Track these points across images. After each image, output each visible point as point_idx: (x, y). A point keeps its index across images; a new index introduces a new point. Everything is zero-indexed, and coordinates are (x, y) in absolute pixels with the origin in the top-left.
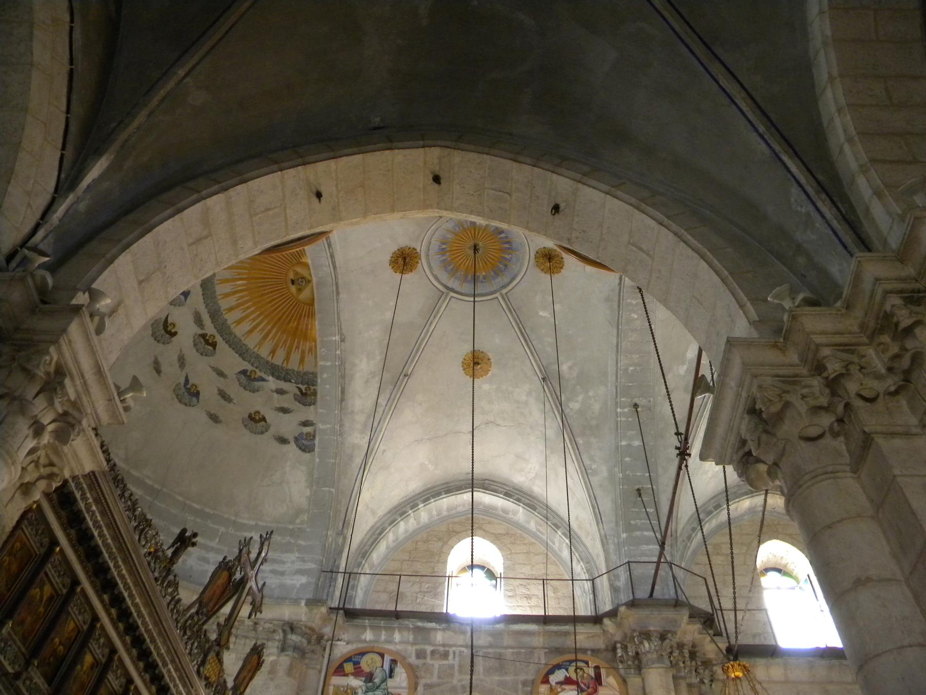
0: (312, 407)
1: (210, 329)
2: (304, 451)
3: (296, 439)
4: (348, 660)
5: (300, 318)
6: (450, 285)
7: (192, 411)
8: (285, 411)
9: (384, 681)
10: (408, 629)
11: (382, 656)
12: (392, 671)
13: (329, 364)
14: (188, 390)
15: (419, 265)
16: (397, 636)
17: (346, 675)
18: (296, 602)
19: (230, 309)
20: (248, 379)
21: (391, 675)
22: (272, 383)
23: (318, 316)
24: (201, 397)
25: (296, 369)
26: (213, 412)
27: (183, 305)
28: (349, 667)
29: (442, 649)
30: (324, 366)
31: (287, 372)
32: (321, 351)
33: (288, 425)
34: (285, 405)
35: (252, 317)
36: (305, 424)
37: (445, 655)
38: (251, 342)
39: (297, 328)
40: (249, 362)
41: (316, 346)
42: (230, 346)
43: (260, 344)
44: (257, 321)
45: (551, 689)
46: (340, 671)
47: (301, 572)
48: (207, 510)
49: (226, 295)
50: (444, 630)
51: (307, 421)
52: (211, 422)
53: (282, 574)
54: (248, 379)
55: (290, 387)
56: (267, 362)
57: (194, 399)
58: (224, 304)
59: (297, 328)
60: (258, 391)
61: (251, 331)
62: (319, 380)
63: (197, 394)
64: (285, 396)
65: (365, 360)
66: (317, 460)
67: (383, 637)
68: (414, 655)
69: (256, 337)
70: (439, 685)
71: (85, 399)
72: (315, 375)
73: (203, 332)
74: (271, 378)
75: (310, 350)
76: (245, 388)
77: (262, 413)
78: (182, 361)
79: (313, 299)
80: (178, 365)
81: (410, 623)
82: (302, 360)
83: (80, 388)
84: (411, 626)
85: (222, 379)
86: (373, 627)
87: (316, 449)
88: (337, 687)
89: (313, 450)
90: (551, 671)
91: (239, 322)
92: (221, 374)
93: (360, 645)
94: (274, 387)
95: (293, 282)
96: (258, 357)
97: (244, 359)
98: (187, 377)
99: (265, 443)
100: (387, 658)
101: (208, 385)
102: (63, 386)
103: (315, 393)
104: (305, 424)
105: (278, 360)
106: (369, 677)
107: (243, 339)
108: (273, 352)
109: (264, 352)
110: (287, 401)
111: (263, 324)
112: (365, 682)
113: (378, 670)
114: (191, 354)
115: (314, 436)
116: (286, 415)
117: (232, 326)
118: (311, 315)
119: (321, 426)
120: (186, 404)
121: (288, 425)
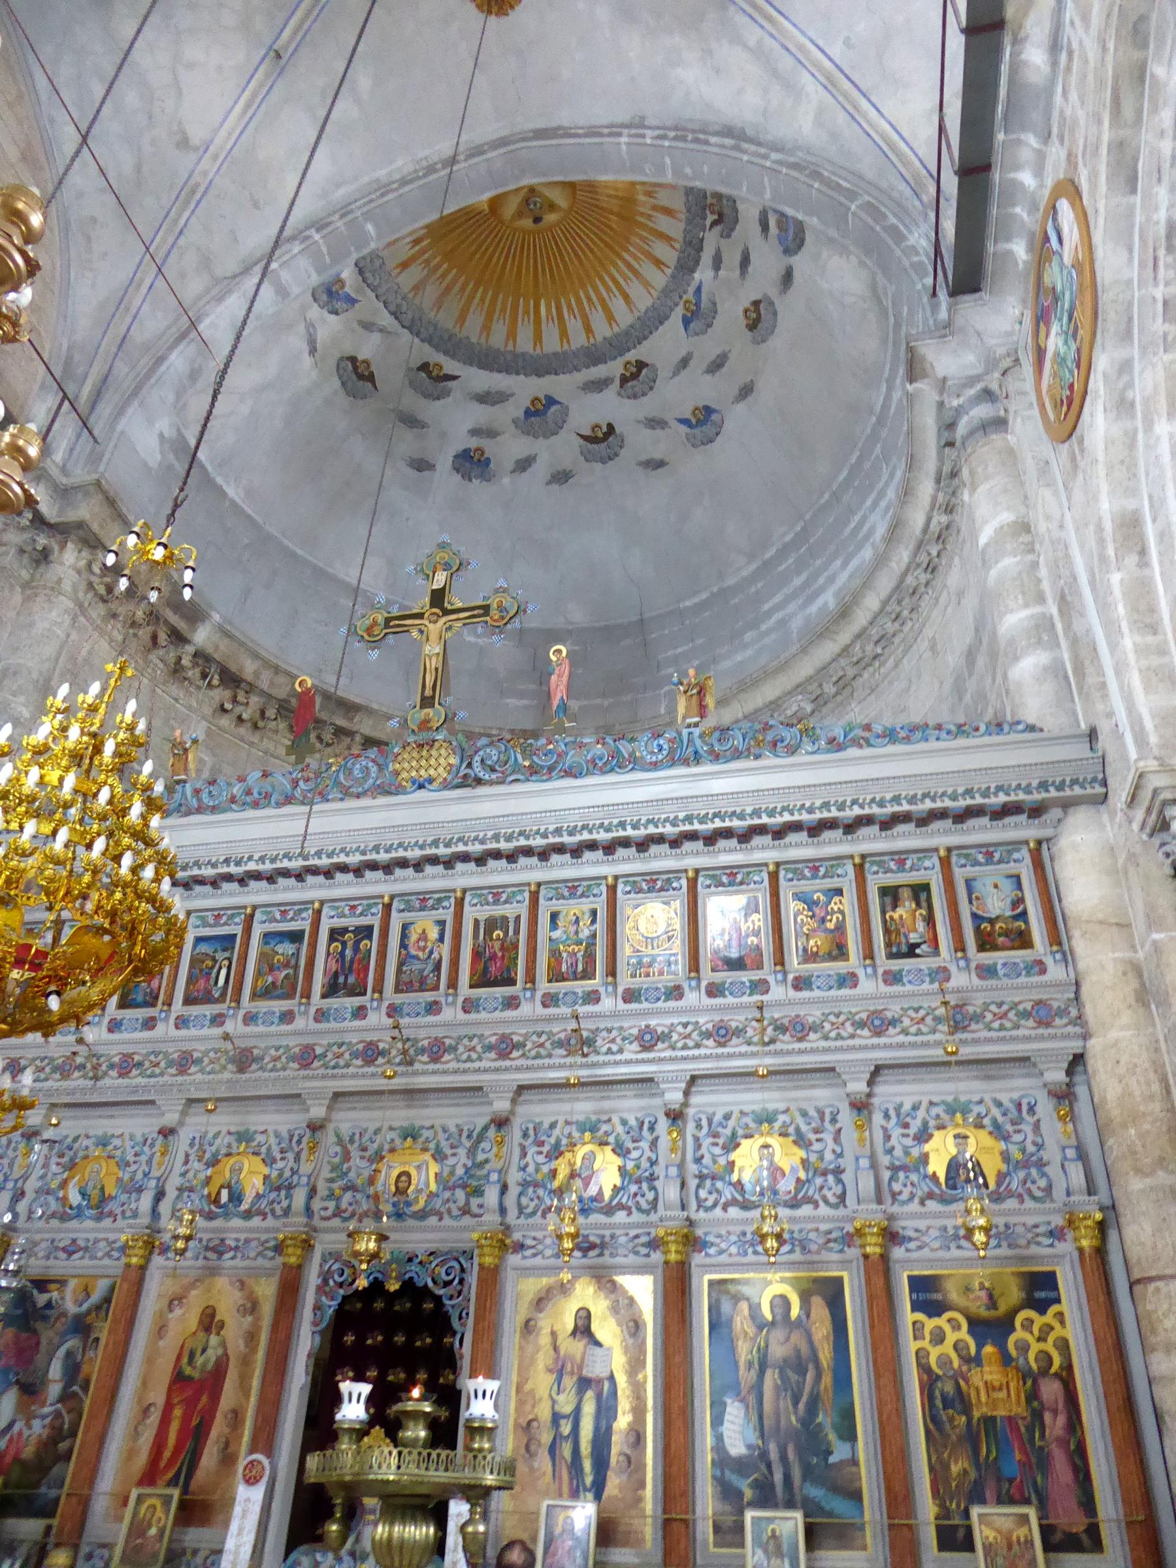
1: (615, 368)
2: (802, 241)
3: (787, 252)
7: (728, 426)
8: (745, 261)
13: (668, 160)
14: (700, 423)
16: (1027, 178)
19: (588, 329)
20: (697, 316)
22: (703, 274)
23: (591, 176)
26: (736, 392)
27: (567, 408)
30: (673, 170)
31: (688, 243)
32: (648, 175)
33: (767, 260)
36: (765, 227)
38: (644, 301)
40: (672, 310)
41: (643, 183)
42: (645, 338)
43: (646, 284)
44: (611, 284)
49: (564, 334)
50: (1016, 41)
52: (750, 399)
55: (711, 239)
56: (673, 276)
57: (714, 417)
58: (578, 339)
59: (618, 215)
60: (714, 304)
61: (626, 297)
62: (698, 184)
63: (708, 410)
65: (680, 70)
66: (815, 220)
69: (635, 289)
72: (689, 191)
73: (617, 382)
74: (697, 275)
75: (649, 194)
76: (710, 325)
77: (747, 305)
78: (655, 423)
80: (659, 432)
82: (668, 212)
85: (692, 363)
87: (800, 217)
91: (610, 318)
92: (684, 362)
94: (710, 273)
95: (537, 220)
96: (666, 292)
97: (667, 318)
99: (790, 311)
101: (699, 389)
103: (718, 196)
104: (765, 227)
105: (669, 255)
107: (637, 314)
108: (658, 263)
109: (659, 279)
114: (648, 405)
115: (783, 215)
117: (616, 329)
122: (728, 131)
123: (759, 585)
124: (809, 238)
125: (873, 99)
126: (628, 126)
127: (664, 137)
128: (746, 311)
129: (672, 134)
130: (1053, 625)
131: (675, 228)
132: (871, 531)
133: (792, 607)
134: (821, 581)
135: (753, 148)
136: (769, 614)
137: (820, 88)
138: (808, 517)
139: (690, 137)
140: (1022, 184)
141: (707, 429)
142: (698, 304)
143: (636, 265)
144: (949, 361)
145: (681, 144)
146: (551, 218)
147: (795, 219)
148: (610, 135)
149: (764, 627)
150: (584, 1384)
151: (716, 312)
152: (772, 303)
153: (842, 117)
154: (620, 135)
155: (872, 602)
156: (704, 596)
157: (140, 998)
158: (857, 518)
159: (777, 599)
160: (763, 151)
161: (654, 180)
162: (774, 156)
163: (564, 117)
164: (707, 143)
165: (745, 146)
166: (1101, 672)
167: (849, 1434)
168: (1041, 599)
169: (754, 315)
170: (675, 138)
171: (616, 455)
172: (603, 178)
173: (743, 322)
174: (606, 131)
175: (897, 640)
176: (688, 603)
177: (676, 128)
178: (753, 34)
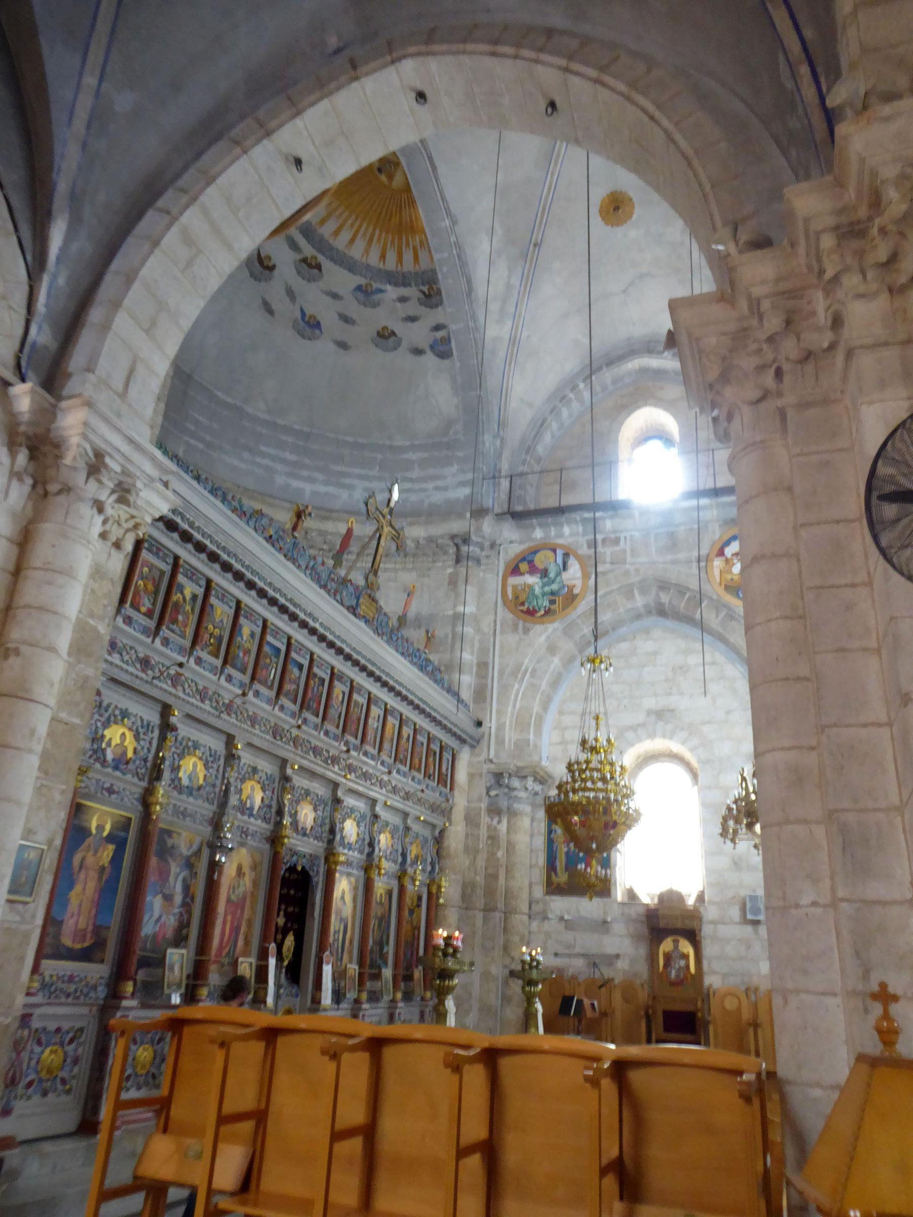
0: (440, 308)
1: (308, 251)
4: (523, 559)
5: (401, 209)
8: (412, 319)
9: (558, 574)
10: (576, 522)
11: (554, 551)
13: (446, 255)
14: (308, 323)
16: (566, 530)
17: (522, 574)
18: (461, 516)
20: (365, 294)
21: (565, 567)
22: (392, 292)
25: (412, 270)
28: (524, 567)
30: (441, 259)
31: (404, 276)
34: (411, 313)
35: (350, 222)
37: (617, 541)
38: (356, 252)
39: (401, 224)
40: (361, 275)
42: (335, 262)
43: (367, 251)
45: (727, 561)
46: (515, 571)
47: (462, 484)
48: (361, 440)
50: (612, 517)
52: (341, 350)
53: (446, 489)
55: (412, 292)
56: (380, 270)
57: (317, 332)
59: (401, 224)
61: (352, 241)
62: (440, 277)
63: (318, 325)
64: (408, 304)
66: (458, 365)
68: (585, 546)
69: (360, 244)
70: (612, 571)
71: (129, 466)
72: (434, 272)
74: (388, 287)
75: (421, 243)
76: (365, 305)
79: (408, 184)
80: (287, 299)
81: (577, 516)
82: (416, 258)
83: (121, 460)
84: (578, 518)
86: (541, 526)
88: (515, 587)
90: (727, 543)
91: (336, 233)
92: (335, 296)
93: (531, 544)
94: (394, 296)
96: (368, 267)
98: (302, 311)
99: (402, 358)
100: (560, 552)
102: (106, 466)
103: (439, 292)
104: (437, 328)
105: (391, 263)
106: (545, 573)
108: (383, 257)
109: (373, 259)
110: (413, 308)
112: (541, 578)
113: (552, 565)
114: (298, 283)
116: (416, 323)
117: (331, 241)
118: (412, 203)
119: (453, 327)
120: (310, 339)
121: (418, 334)
122: (469, 282)
123: (264, 431)
124: (446, 362)
128: (385, 328)
131: (408, 265)
133: (279, 467)
134: (305, 473)
136: (264, 455)
137: (508, 336)
141: (308, 330)
142: (372, 293)
144: (488, 526)
146: (383, 178)
149: (258, 460)
150: (341, 919)
152: (399, 345)
153: (502, 354)
156: (230, 400)
157: (239, 665)
159: (272, 451)
161: (431, 245)
163: (442, 170)
167: (388, 943)
169: (386, 334)
171: (260, 281)
172: (420, 209)
176: (219, 394)
178: (515, 281)
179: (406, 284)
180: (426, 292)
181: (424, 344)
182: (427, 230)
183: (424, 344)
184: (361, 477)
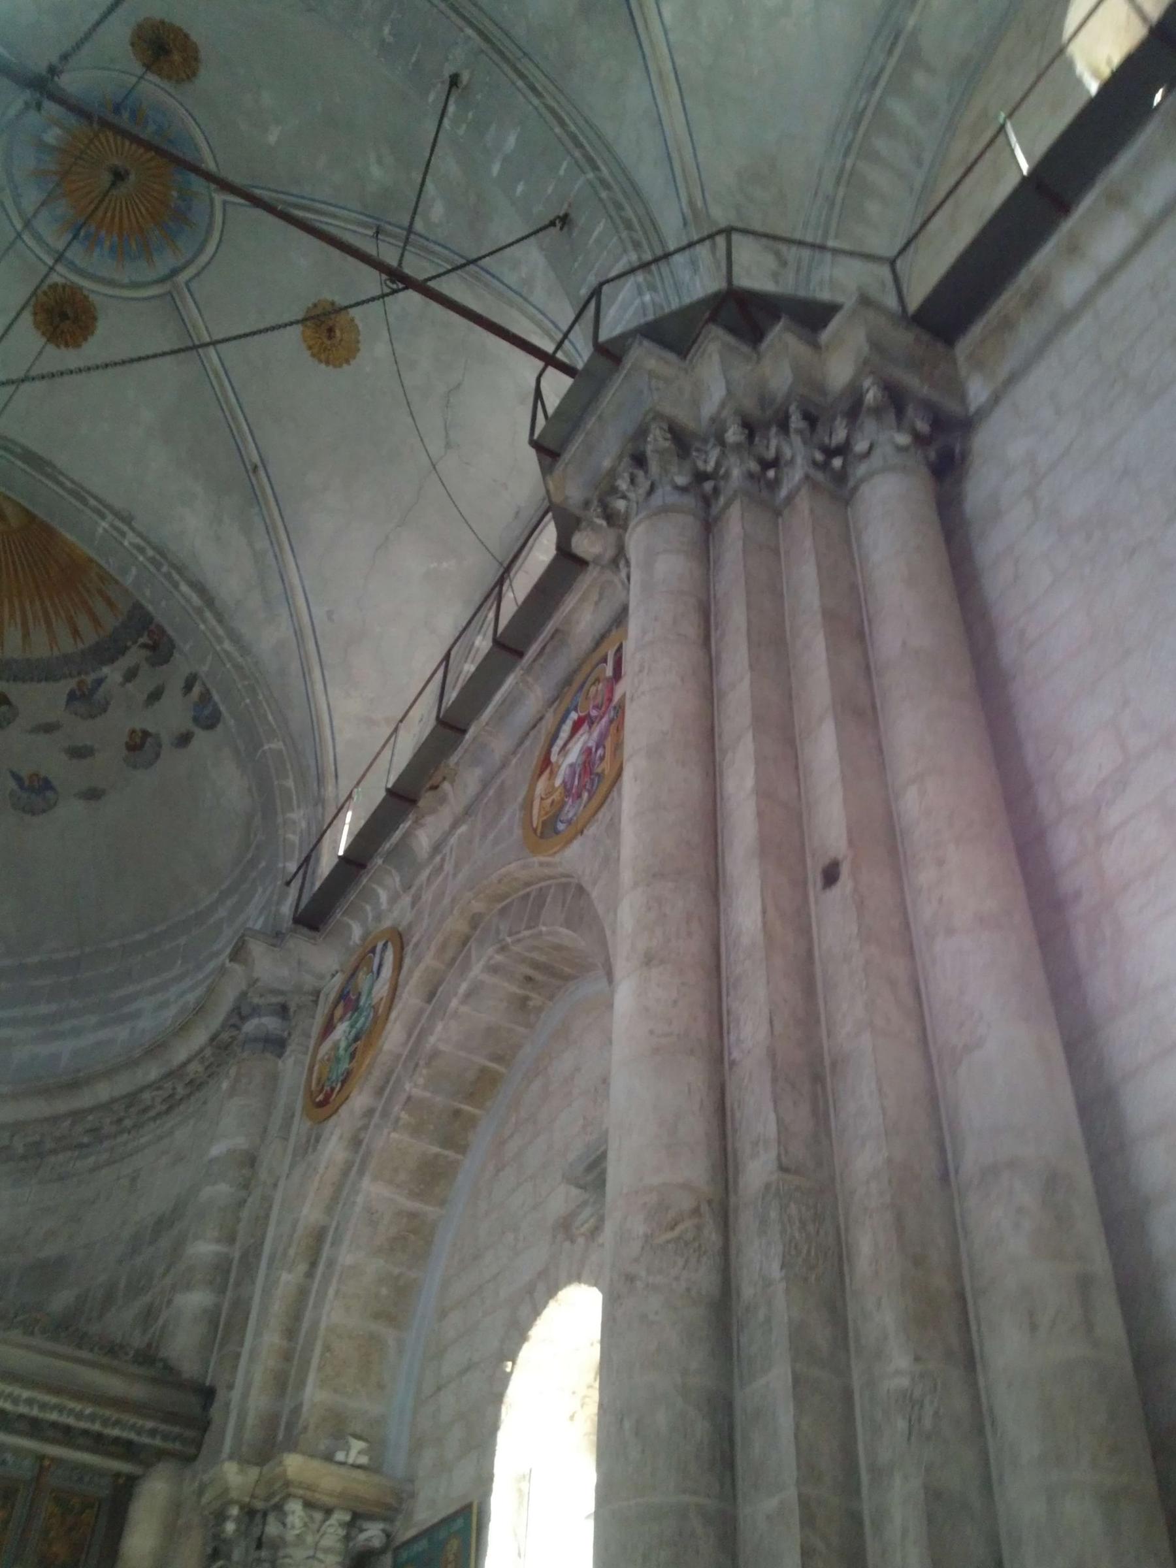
0: (176, 655)
3: (196, 720)
6: (162, 269)
8: (155, 696)
12: (380, 966)
13: (134, 571)
15: (92, 297)
16: (383, 896)
20: (86, 700)
22: (112, 674)
24: (55, 783)
29: (438, 859)
34: (151, 687)
36: (188, 687)
38: (41, 650)
42: (24, 681)
48: (157, 930)
50: (417, 823)
51: (187, 681)
54: (86, 700)
55: (135, 656)
57: (49, 794)
60: (108, 703)
61: (26, 635)
62: (150, 608)
63: (47, 785)
66: (232, 722)
67: (370, 916)
72: (138, 606)
74: (106, 670)
76: (92, 716)
82: (110, 603)
87: (222, 708)
89: (220, 713)
92: (48, 728)
101: (49, 760)
103: (163, 632)
104: (188, 687)
105: (90, 636)
108: (76, 633)
109: (67, 645)
111: (28, 607)
115: (208, 690)
118: (48, 531)
120: (44, 811)
122: (200, 588)
124: (220, 727)
125: (326, 672)
126: (117, 514)
127: (141, 550)
128: (133, 732)
129: (150, 553)
130: (228, 1271)
131: (111, 622)
132: (137, 1015)
135: (214, 622)
137: (292, 630)
138: (87, 950)
139: (165, 569)
140: (377, 897)
143: (53, 616)
145: (152, 568)
147: (215, 704)
148: (95, 510)
151: (105, 710)
152: (160, 746)
154: (103, 517)
155: (103, 1092)
158: (131, 989)
160: (220, 631)
162: (227, 645)
164: (176, 586)
165: (208, 614)
166: (241, 1343)
168: (231, 1239)
170: (152, 560)
172: (68, 536)
173: (126, 739)
174: (92, 502)
175: (106, 1144)
177: (154, 548)
178: (262, 544)
179: (123, 651)
180: (150, 642)
181: (190, 725)
182: (93, 554)
183: (190, 725)
184: (152, 991)
